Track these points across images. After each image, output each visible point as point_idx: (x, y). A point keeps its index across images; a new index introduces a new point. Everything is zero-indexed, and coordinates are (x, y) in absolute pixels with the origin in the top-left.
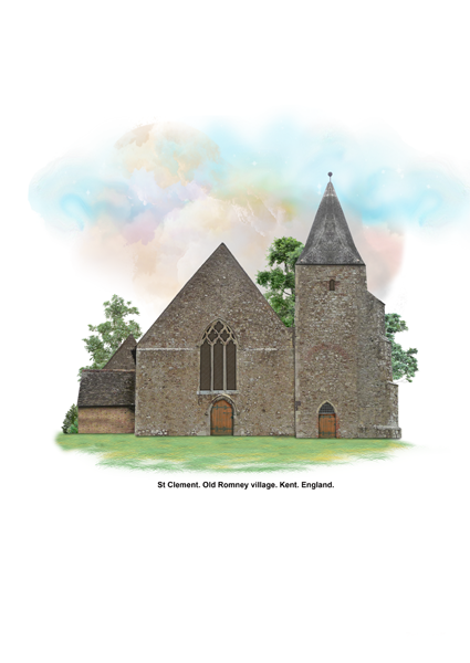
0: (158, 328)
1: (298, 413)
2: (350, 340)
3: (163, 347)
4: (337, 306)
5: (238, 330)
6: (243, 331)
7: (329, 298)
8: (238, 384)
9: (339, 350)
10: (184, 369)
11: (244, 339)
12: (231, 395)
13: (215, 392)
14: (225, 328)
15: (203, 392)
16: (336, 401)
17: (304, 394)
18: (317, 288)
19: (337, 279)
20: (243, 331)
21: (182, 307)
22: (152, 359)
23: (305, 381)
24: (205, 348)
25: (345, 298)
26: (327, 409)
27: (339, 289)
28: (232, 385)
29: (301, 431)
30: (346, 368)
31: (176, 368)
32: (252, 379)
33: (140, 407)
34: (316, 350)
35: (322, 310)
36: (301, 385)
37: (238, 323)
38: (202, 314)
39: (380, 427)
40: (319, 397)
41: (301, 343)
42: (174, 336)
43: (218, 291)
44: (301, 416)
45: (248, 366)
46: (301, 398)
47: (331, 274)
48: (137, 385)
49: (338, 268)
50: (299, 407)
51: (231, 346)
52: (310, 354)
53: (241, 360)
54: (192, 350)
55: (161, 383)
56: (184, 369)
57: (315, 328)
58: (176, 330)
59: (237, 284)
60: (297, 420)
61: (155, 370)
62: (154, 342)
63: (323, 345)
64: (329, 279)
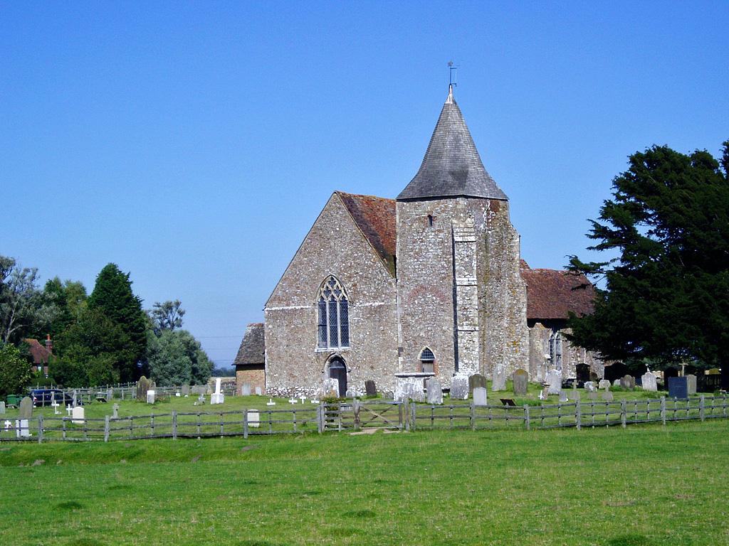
1: (401, 359)
3: (287, 305)
4: (434, 244)
5: (350, 285)
6: (355, 285)
7: (427, 236)
9: (435, 291)
10: (304, 328)
11: (356, 293)
15: (322, 350)
17: (406, 339)
19: (434, 215)
20: (355, 285)
23: (406, 326)
24: (323, 307)
25: (441, 235)
26: (427, 353)
27: (436, 224)
28: (345, 341)
30: (443, 311)
32: (361, 336)
35: (420, 249)
36: (403, 330)
38: (319, 270)
41: (402, 287)
43: (332, 244)
44: (403, 363)
45: (358, 322)
48: (266, 345)
52: (409, 300)
54: (310, 307)
55: (285, 342)
56: (304, 328)
58: (298, 288)
62: (280, 300)
63: (422, 287)
64: (426, 215)
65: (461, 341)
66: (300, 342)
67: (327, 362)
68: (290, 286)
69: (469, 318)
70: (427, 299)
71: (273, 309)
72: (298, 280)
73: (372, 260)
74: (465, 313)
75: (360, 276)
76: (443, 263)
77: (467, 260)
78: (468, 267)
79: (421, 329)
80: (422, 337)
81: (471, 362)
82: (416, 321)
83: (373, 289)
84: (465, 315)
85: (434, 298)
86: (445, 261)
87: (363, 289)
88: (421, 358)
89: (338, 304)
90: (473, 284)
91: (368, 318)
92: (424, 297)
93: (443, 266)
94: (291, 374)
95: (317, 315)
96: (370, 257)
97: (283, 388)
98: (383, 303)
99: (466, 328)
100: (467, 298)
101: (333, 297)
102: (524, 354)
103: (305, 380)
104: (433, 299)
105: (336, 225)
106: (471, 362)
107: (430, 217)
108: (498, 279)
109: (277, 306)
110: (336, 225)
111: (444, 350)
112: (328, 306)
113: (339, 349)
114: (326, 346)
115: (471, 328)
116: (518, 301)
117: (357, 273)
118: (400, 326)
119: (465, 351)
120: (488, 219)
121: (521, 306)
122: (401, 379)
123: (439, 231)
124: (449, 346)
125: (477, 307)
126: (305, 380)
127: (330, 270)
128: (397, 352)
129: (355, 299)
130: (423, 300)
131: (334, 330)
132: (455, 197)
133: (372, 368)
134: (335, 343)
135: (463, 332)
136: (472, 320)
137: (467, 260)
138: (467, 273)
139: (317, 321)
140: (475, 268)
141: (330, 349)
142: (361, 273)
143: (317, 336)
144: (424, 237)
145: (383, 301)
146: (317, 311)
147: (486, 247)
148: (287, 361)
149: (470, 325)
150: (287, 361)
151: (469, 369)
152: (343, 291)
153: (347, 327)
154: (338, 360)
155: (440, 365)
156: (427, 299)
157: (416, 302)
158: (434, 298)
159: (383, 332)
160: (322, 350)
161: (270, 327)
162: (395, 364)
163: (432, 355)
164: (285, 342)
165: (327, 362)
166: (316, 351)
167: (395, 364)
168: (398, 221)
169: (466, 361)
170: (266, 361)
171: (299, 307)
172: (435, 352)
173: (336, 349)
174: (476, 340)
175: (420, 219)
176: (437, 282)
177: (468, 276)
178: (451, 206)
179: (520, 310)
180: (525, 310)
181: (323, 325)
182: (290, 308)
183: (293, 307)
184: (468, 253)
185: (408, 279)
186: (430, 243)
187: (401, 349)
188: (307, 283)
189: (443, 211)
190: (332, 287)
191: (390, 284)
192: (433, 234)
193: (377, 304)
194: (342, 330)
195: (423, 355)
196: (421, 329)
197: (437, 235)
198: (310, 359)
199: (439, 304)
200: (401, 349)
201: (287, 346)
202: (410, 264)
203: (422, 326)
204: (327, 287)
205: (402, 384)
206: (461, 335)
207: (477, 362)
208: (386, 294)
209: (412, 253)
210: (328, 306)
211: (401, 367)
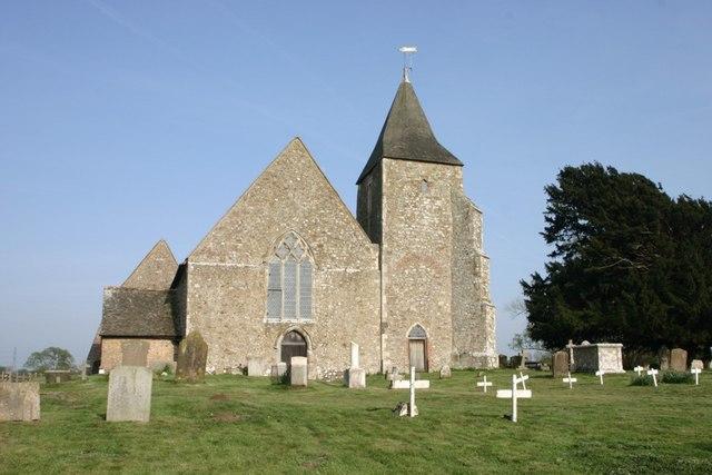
1: (385, 336)
2: (443, 252)
3: (222, 261)
4: (430, 210)
5: (314, 245)
7: (421, 202)
9: (431, 262)
12: (307, 325)
16: (427, 323)
17: (391, 313)
25: (438, 203)
28: (306, 312)
29: (388, 358)
30: (440, 284)
34: (407, 261)
35: (413, 214)
37: (315, 237)
38: (271, 223)
39: (475, 354)
41: (390, 253)
42: (235, 248)
46: (387, 319)
50: (387, 330)
52: (400, 266)
55: (218, 308)
58: (239, 241)
60: (384, 346)
62: (211, 254)
63: (414, 255)
66: (240, 311)
67: (282, 337)
68: (228, 237)
79: (411, 303)
91: (341, 286)
93: (440, 236)
113: (298, 322)
114: (278, 315)
123: (437, 198)
131: (291, 295)
133: (344, 345)
141: (284, 321)
157: (406, 271)
160: (274, 321)
161: (197, 286)
166: (265, 321)
168: (384, 181)
187: (383, 326)
191: (368, 249)
196: (411, 303)
202: (400, 229)
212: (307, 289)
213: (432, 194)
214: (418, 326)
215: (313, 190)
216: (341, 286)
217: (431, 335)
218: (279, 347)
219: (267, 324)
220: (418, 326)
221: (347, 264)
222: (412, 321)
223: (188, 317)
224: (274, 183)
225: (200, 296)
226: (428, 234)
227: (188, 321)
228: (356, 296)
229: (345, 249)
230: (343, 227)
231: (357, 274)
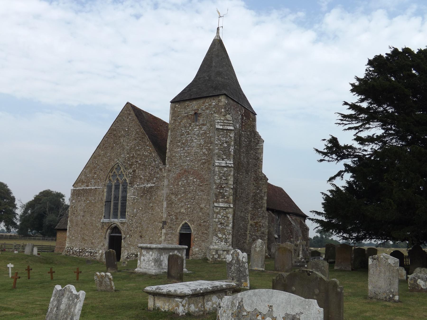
0: (85, 172)
1: (164, 231)
3: (87, 186)
4: (198, 135)
6: (134, 171)
8: (127, 214)
11: (134, 177)
12: (121, 223)
13: (112, 220)
14: (122, 169)
15: (106, 220)
16: (192, 221)
17: (169, 215)
18: (184, 121)
20: (134, 171)
21: (100, 156)
22: (79, 196)
23: (170, 204)
24: (109, 188)
25: (204, 128)
28: (123, 215)
30: (202, 191)
31: (91, 202)
33: (70, 230)
34: (179, 178)
36: (167, 207)
37: (131, 165)
40: (180, 217)
41: (169, 171)
42: (93, 178)
44: (166, 234)
47: (196, 107)
48: (69, 215)
49: (201, 101)
50: (166, 226)
51: (125, 185)
53: (130, 195)
55: (82, 213)
57: (180, 156)
58: (95, 173)
59: (134, 133)
61: (80, 204)
62: (83, 182)
64: (193, 113)
65: (216, 216)
66: (92, 215)
69: (225, 196)
70: (189, 181)
71: (78, 188)
72: (96, 167)
73: (149, 152)
74: (221, 191)
75: (139, 163)
76: (204, 150)
77: (225, 145)
78: (226, 153)
79: (182, 207)
80: (183, 213)
81: (224, 236)
82: (179, 199)
83: (147, 174)
84: (221, 193)
85: (195, 180)
86: (206, 149)
87: (140, 174)
88: (180, 231)
89: (121, 185)
90: (230, 165)
91: (142, 196)
92: (186, 179)
93: (204, 153)
94: (83, 238)
95: (105, 194)
96: (148, 150)
97: (77, 248)
98: (153, 185)
99: (221, 205)
100: (223, 178)
101: (118, 180)
102: (263, 233)
103: (92, 243)
104: (194, 181)
105: (126, 126)
106: (224, 236)
107: (195, 113)
108: (247, 172)
109: (80, 186)
110: (126, 126)
111: (200, 225)
112: (113, 187)
113: (117, 221)
115: (226, 205)
116: (261, 191)
117: (137, 162)
118: (165, 204)
119: (219, 226)
120: (242, 122)
121: (263, 195)
122: (144, 252)
123: (203, 125)
124: (204, 222)
125: (232, 187)
126: (92, 243)
127: (118, 160)
128: (161, 225)
129: (134, 181)
130: (185, 181)
131: (116, 205)
132: (218, 96)
133: (141, 237)
134: (116, 216)
135: (219, 209)
136: (228, 198)
137: (225, 145)
138: (224, 157)
139: (105, 198)
140: (232, 153)
141: (112, 220)
142: (140, 162)
143: (104, 209)
144: (190, 130)
145: (154, 183)
146: (105, 190)
147: (239, 143)
148: (81, 228)
149: (226, 202)
150: (81, 228)
151: (223, 243)
152: (125, 175)
153: (126, 203)
154: (116, 229)
155: (196, 238)
156: (189, 181)
157: (180, 183)
158: (195, 180)
159: (152, 208)
160: (106, 220)
162: (159, 234)
163: (190, 229)
164: (82, 213)
165: (109, 230)
166: (102, 221)
167: (159, 234)
169: (220, 236)
170: (68, 227)
171: (94, 188)
172: (192, 227)
173: (116, 220)
174: (230, 216)
175: (188, 116)
176: (198, 167)
177: (226, 160)
178: (214, 104)
179: (262, 198)
180: (266, 198)
181: (108, 202)
182: (88, 188)
183: (90, 188)
184: (227, 140)
185: (175, 165)
186: (194, 135)
188: (102, 170)
189: (207, 109)
190: (118, 172)
191: (161, 170)
192: (198, 127)
193: (149, 185)
194: (121, 206)
195: (182, 228)
196: (182, 207)
197: (201, 128)
198: (97, 227)
199: (199, 185)
200: (165, 223)
201: (83, 216)
202: (176, 152)
203: (183, 204)
204: (115, 172)
205: (145, 258)
206: (217, 211)
207: (230, 237)
208: (157, 178)
209: (179, 144)
210: (113, 187)
211: (163, 238)
212: (124, 199)
213: (201, 122)
214: (186, 223)
215: (134, 135)
216: (142, 196)
217: (194, 230)
218: (107, 237)
219: (103, 222)
220: (186, 223)
221: (148, 181)
222: (182, 220)
223: (69, 219)
224: (114, 135)
225: (75, 207)
226: (196, 153)
227: (69, 222)
228: (150, 203)
229: (148, 170)
230: (146, 156)
231: (151, 187)
